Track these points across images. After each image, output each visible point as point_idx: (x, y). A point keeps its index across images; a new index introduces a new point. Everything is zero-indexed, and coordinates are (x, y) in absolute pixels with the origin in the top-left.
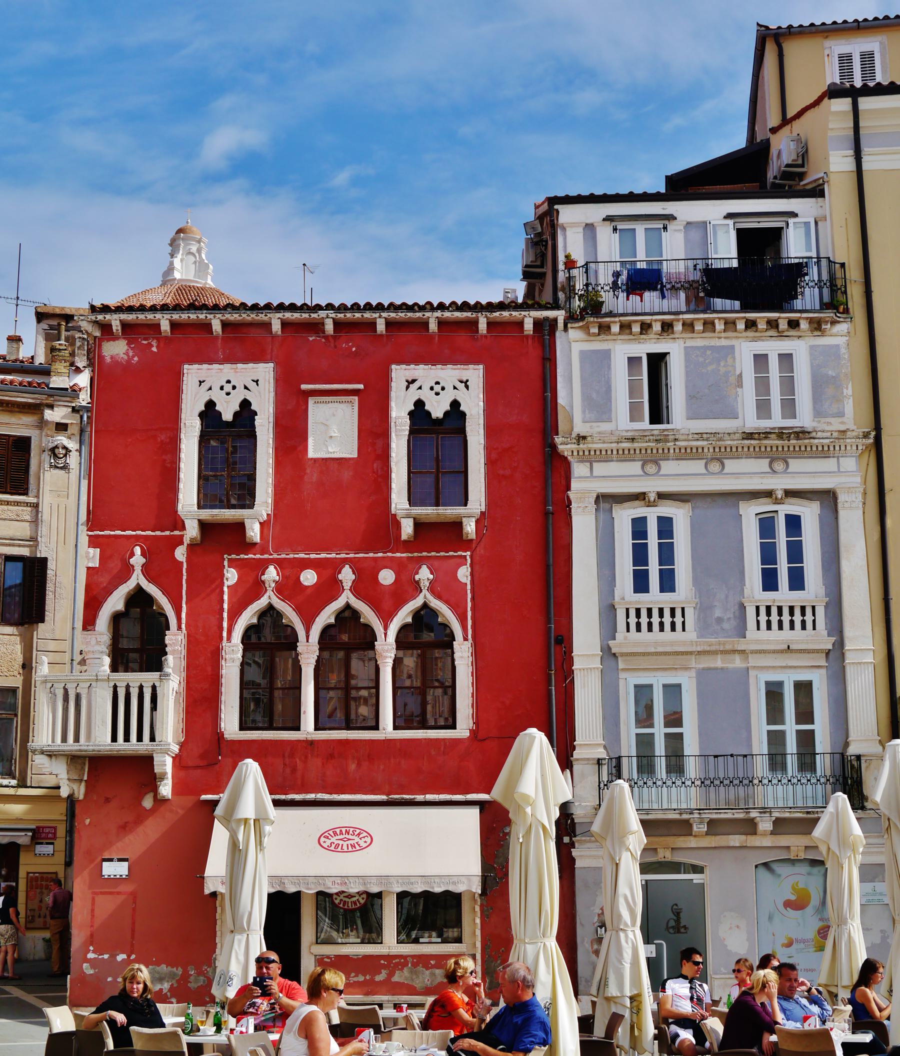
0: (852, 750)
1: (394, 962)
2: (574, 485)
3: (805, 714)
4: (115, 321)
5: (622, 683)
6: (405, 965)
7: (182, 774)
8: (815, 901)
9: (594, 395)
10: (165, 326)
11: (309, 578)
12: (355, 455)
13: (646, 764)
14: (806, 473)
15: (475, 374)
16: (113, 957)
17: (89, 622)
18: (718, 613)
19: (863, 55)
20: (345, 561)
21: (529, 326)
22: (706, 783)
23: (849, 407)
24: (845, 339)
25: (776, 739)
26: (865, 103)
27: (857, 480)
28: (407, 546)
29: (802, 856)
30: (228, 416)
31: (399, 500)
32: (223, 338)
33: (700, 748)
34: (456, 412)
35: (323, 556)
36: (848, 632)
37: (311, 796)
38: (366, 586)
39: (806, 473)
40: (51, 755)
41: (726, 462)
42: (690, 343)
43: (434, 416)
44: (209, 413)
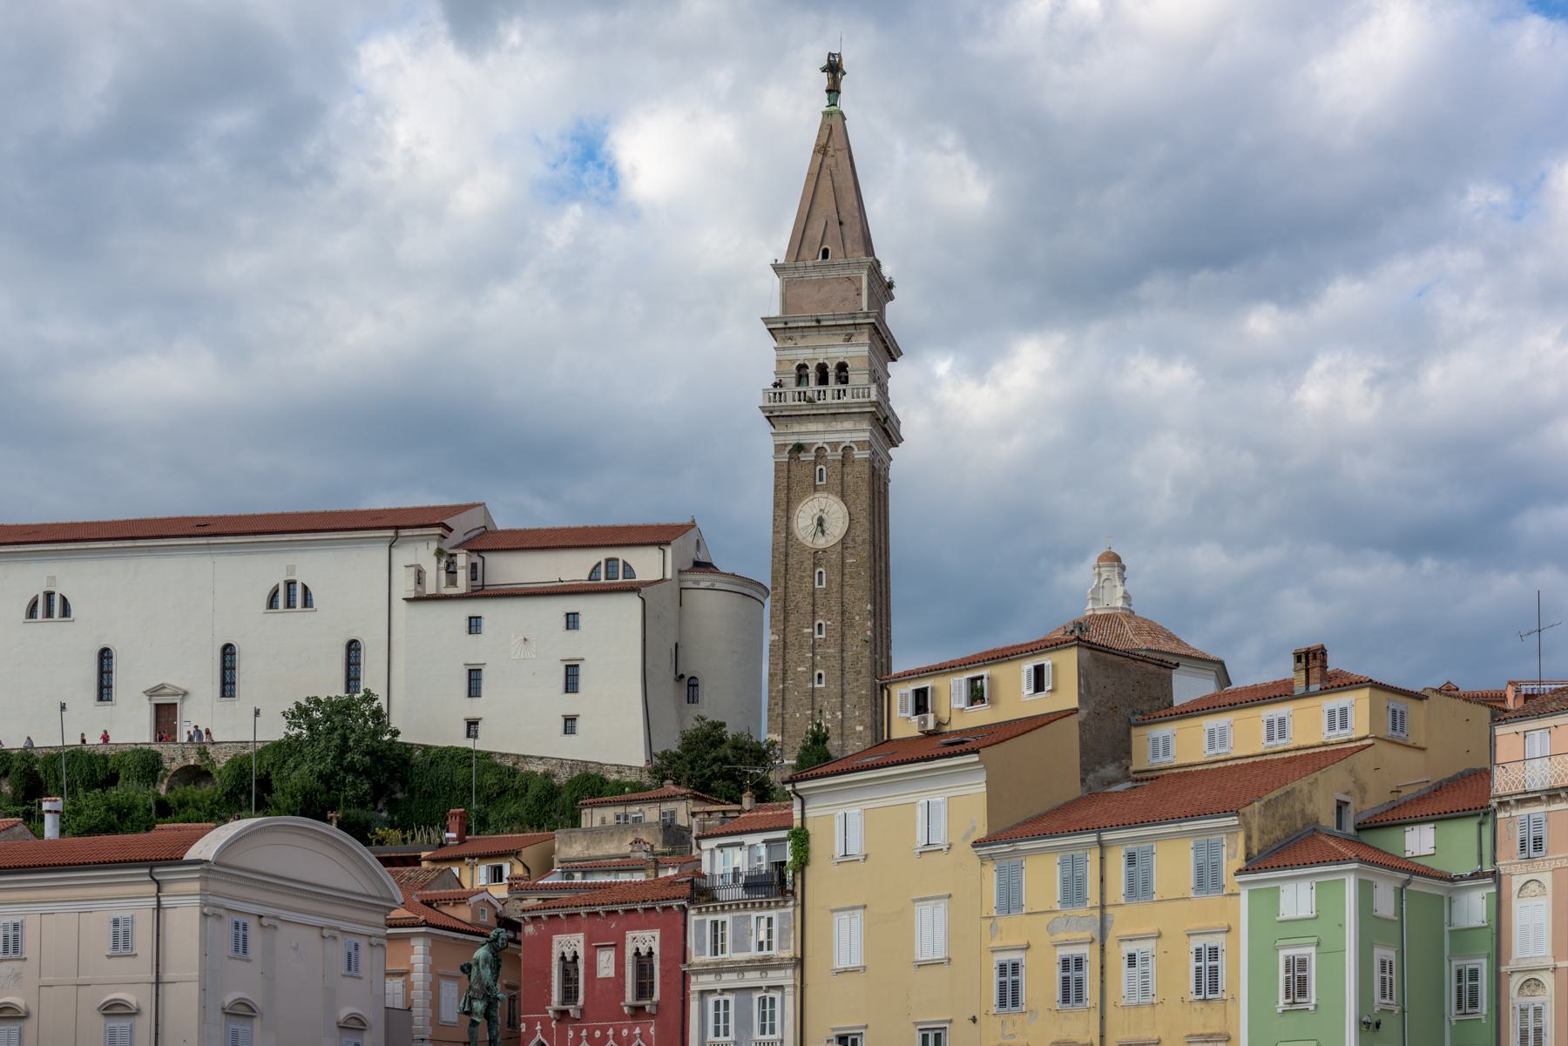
2: (692, 988)
11: (598, 1034)
15: (657, 933)
27: (791, 982)
30: (569, 959)
39: (775, 977)
44: (563, 958)
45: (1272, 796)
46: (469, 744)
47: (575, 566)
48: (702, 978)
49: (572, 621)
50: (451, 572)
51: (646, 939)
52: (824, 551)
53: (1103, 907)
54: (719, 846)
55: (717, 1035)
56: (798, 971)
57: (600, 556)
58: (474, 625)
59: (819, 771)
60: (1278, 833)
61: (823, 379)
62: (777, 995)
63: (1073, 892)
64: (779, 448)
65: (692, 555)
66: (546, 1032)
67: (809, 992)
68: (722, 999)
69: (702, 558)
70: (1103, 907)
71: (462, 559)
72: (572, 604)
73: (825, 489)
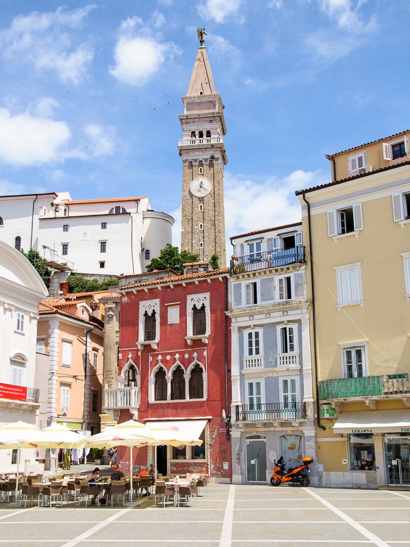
0: (305, 400)
1: (189, 465)
2: (232, 325)
3: (293, 390)
4: (123, 292)
5: (245, 382)
6: (191, 465)
7: (140, 413)
8: (297, 447)
9: (237, 297)
10: (135, 292)
12: (178, 322)
13: (252, 406)
14: (293, 315)
15: (208, 295)
16: (125, 462)
17: (120, 374)
18: (270, 360)
19: (359, 158)
20: (177, 352)
21: (221, 279)
22: (268, 412)
23: (305, 292)
24: (304, 271)
25: (286, 398)
26: (305, 194)
28: (191, 347)
29: (291, 434)
30: (150, 314)
32: (149, 293)
33: (266, 401)
34: (203, 307)
35: (172, 351)
36: (304, 364)
37: (167, 419)
38: (182, 360)
39: (293, 315)
40: (108, 410)
41: (271, 314)
42: (262, 278)
43: (198, 308)
44: (146, 314)
48: (238, 319)
49: (104, 226)
51: (201, 299)
52: (203, 198)
54: (246, 241)
55: (251, 353)
56: (311, 308)
57: (114, 205)
61: (201, 135)
62: (295, 327)
64: (184, 161)
66: (136, 359)
67: (317, 321)
68: (253, 331)
71: (62, 208)
72: (104, 220)
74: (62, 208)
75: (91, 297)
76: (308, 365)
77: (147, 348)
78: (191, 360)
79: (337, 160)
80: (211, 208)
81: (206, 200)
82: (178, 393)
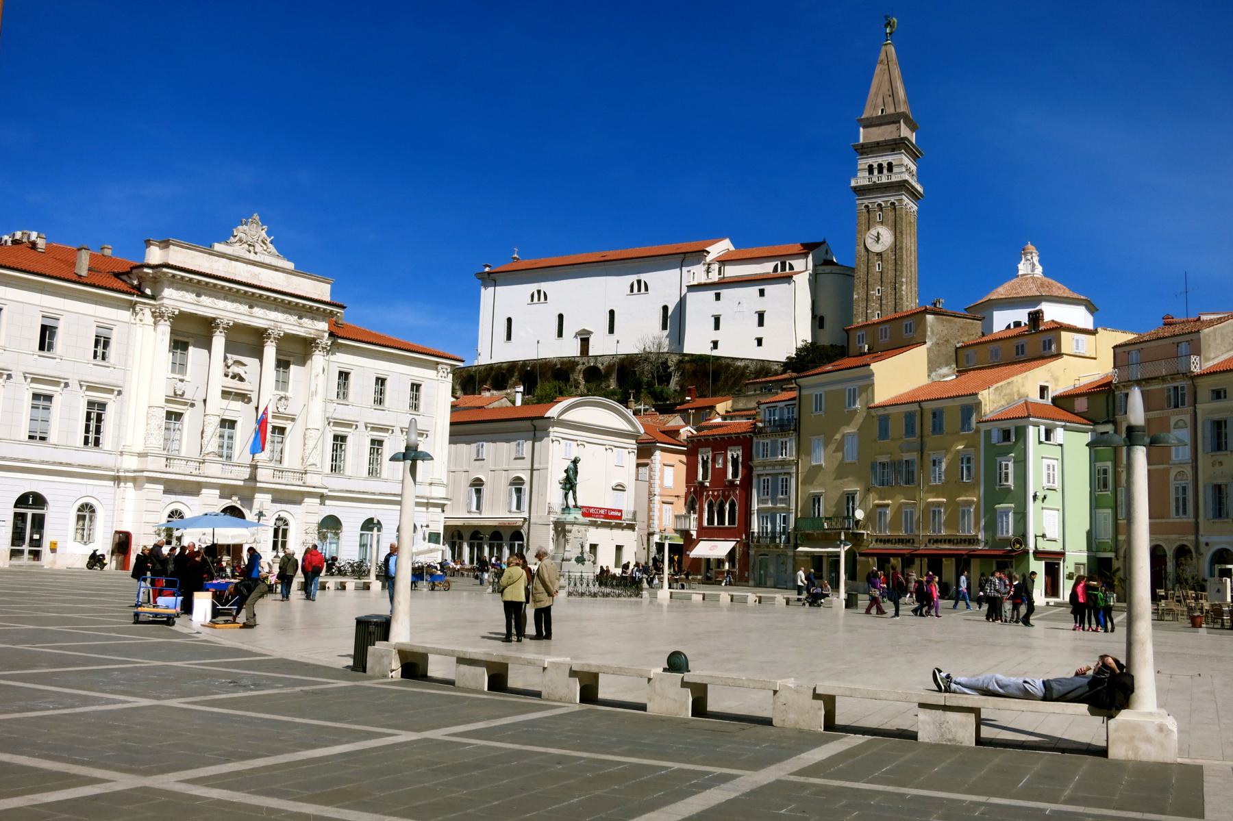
31: (730, 477)
45: (999, 384)
46: (715, 353)
47: (767, 268)
49: (762, 293)
50: (708, 271)
51: (735, 452)
53: (922, 437)
58: (718, 297)
59: (820, 370)
60: (1003, 402)
61: (880, 171)
63: (910, 430)
65: (823, 256)
69: (828, 257)
70: (922, 437)
73: (882, 223)
74: (716, 267)
75: (712, 408)
76: (793, 507)
77: (702, 484)
78: (729, 496)
79: (851, 333)
80: (891, 267)
81: (884, 256)
82: (721, 521)
